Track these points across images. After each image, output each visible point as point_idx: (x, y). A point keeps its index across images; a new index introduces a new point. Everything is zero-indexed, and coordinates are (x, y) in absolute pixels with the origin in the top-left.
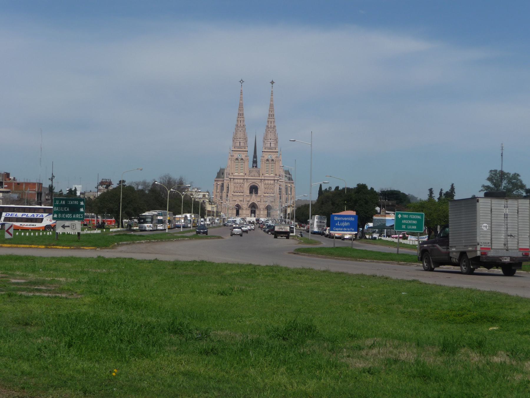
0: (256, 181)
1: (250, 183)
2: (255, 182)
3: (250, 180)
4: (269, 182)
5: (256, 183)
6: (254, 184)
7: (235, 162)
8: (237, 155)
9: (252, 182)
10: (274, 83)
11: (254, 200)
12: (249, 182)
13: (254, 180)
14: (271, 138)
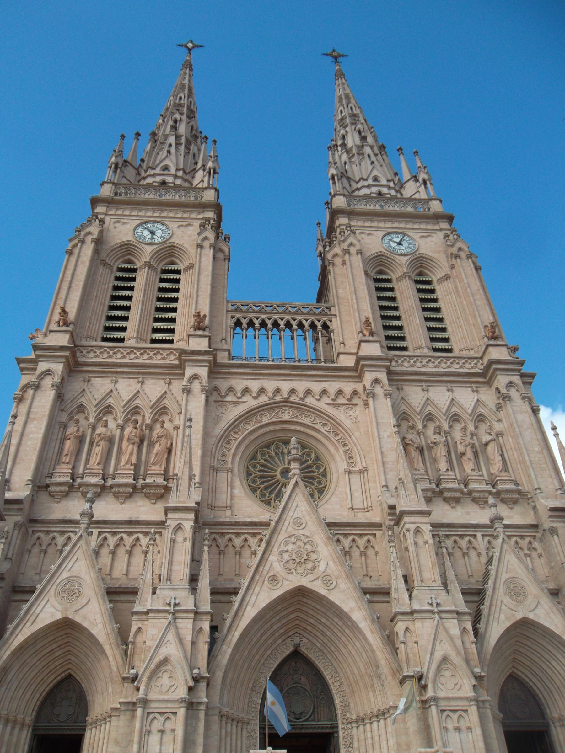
0: (308, 392)
1: (250, 403)
2: (294, 398)
3: (239, 384)
6: (286, 416)
7: (104, 263)
9: (263, 399)
12: (236, 403)
13: (285, 386)
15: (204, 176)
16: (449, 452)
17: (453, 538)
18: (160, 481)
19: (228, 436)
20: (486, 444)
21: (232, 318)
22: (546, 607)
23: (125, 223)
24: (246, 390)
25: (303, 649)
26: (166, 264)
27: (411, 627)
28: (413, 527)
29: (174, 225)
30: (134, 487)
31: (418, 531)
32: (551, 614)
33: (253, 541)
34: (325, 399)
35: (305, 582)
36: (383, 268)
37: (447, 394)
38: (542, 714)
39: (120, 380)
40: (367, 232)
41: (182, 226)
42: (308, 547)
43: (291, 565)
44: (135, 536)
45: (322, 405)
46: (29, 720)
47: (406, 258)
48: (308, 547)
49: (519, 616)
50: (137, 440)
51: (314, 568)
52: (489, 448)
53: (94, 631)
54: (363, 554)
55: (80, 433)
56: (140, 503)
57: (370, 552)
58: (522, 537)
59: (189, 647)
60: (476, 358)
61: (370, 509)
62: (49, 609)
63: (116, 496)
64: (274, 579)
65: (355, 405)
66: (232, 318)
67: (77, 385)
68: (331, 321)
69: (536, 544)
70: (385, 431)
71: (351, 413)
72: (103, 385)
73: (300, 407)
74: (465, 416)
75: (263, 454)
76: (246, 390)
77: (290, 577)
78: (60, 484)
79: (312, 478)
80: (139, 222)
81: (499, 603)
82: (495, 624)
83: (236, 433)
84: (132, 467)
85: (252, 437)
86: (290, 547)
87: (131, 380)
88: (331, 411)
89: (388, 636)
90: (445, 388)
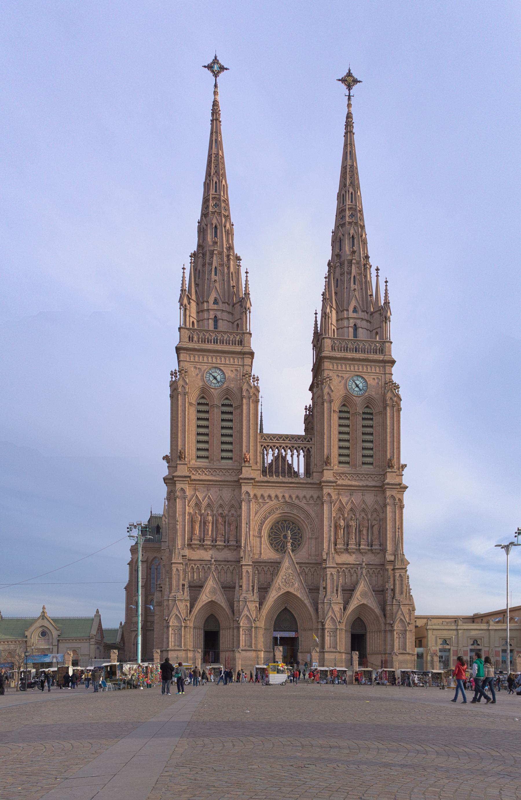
0: (297, 497)
10: (356, 81)
15: (242, 313)
17: (349, 569)
18: (235, 543)
20: (373, 526)
21: (262, 446)
22: (372, 600)
24: (270, 497)
25: (288, 608)
26: (224, 400)
27: (323, 607)
28: (330, 572)
30: (225, 546)
32: (373, 603)
33: (271, 569)
35: (291, 590)
37: (362, 497)
38: (366, 630)
39: (211, 488)
44: (227, 566)
45: (302, 504)
46: (202, 627)
47: (360, 399)
49: (361, 603)
50: (223, 523)
52: (374, 528)
53: (222, 605)
54: (312, 575)
56: (228, 552)
57: (315, 573)
58: (376, 569)
60: (382, 475)
61: (318, 555)
63: (218, 549)
65: (317, 504)
66: (262, 446)
68: (311, 448)
69: (381, 572)
71: (315, 508)
78: (195, 545)
79: (296, 538)
84: (223, 537)
87: (217, 488)
88: (306, 507)
89: (316, 608)
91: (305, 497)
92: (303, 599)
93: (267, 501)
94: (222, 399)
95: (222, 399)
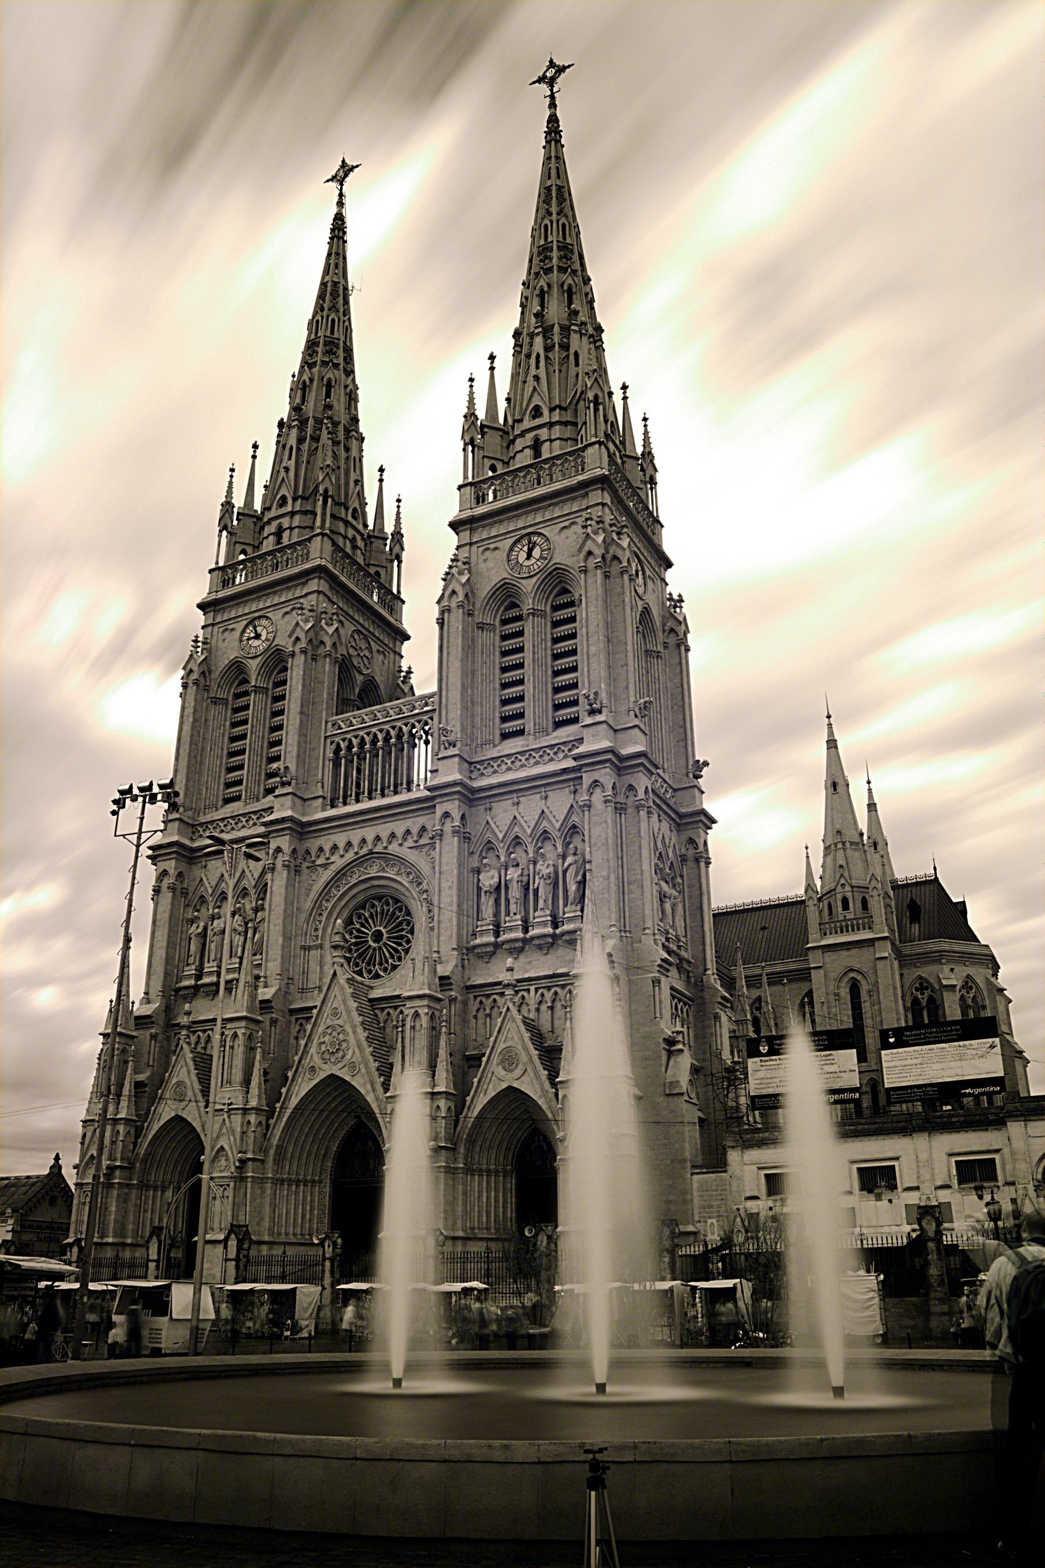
1: (338, 862)
2: (379, 849)
3: (327, 844)
4: (530, 808)
5: (400, 860)
6: (373, 872)
8: (237, 634)
9: (350, 856)
11: (335, 1051)
12: (325, 866)
14: (536, 401)
16: (526, 888)
19: (320, 906)
21: (332, 743)
23: (233, 629)
28: (413, 1011)
29: (276, 616)
31: (416, 1015)
34: (410, 843)
36: (514, 600)
40: (492, 546)
41: (287, 613)
42: (341, 1037)
43: (327, 1056)
45: (405, 852)
47: (534, 580)
48: (341, 1037)
49: (504, 1085)
51: (343, 1057)
55: (200, 930)
59: (238, 1137)
62: (167, 1109)
64: (313, 1069)
67: (198, 872)
68: (432, 719)
70: (448, 881)
72: (217, 868)
73: (386, 857)
74: (555, 834)
75: (359, 916)
76: (335, 848)
77: (325, 1067)
78: (186, 988)
80: (245, 623)
81: (490, 1075)
82: (482, 1095)
83: (327, 900)
85: (343, 903)
86: (327, 1038)
88: (411, 856)
90: (538, 796)
91: (408, 832)
92: (363, 1092)
93: (333, 859)
94: (275, 673)
95: (275, 673)
